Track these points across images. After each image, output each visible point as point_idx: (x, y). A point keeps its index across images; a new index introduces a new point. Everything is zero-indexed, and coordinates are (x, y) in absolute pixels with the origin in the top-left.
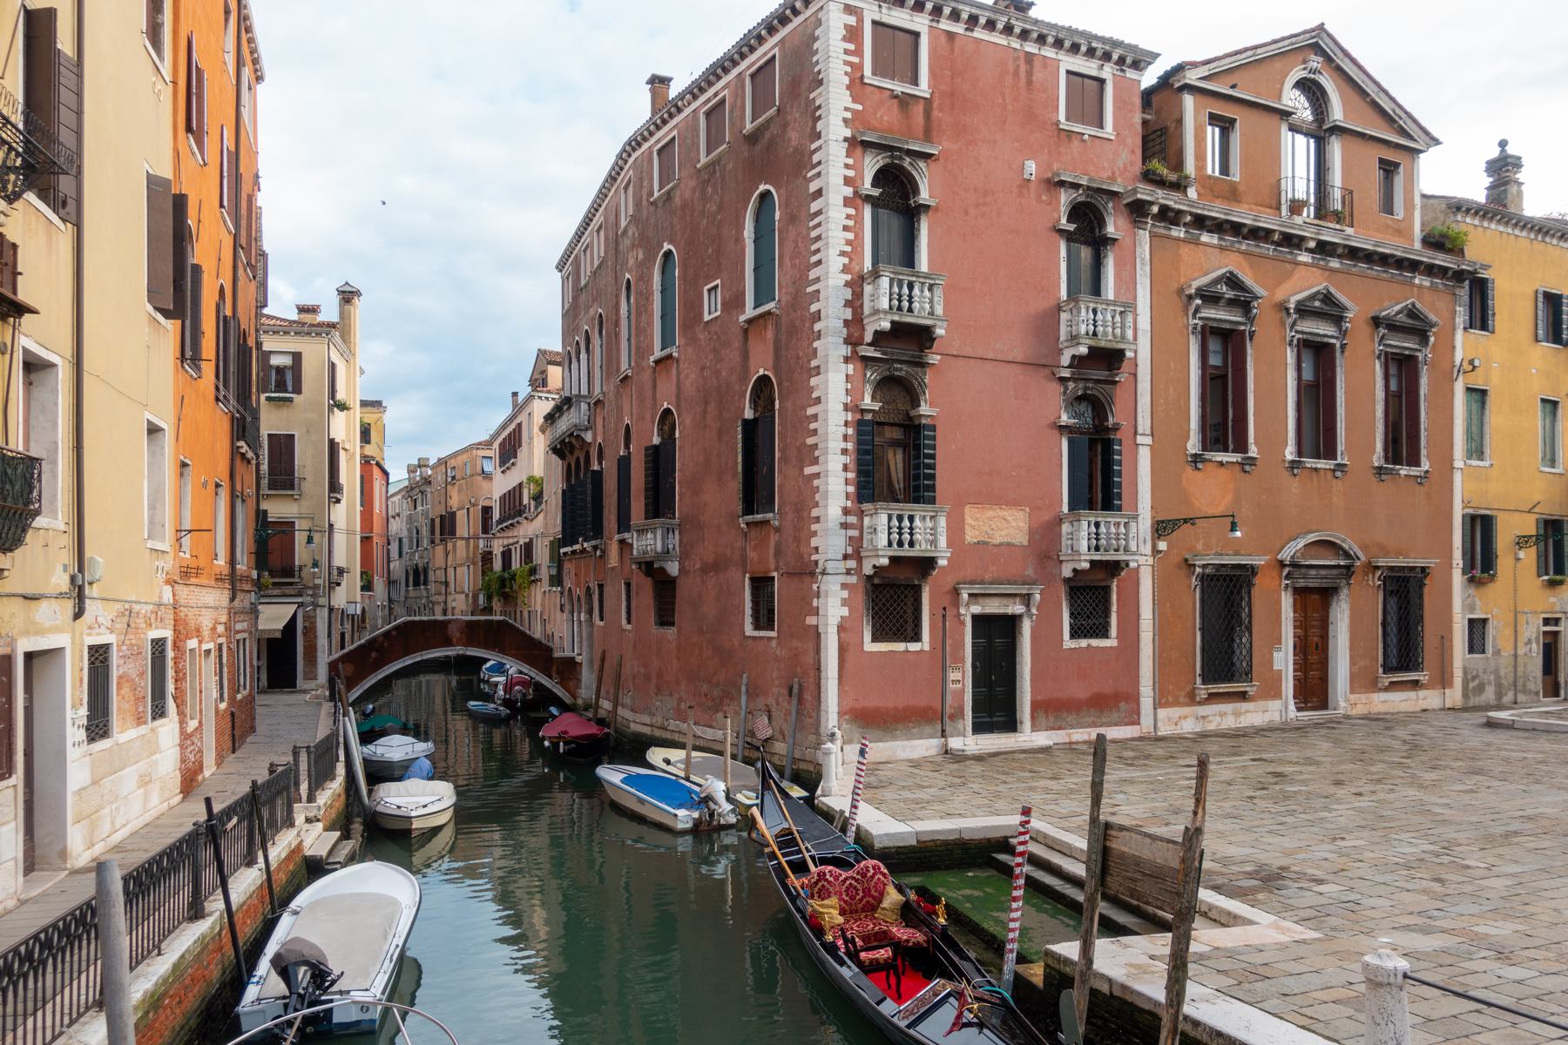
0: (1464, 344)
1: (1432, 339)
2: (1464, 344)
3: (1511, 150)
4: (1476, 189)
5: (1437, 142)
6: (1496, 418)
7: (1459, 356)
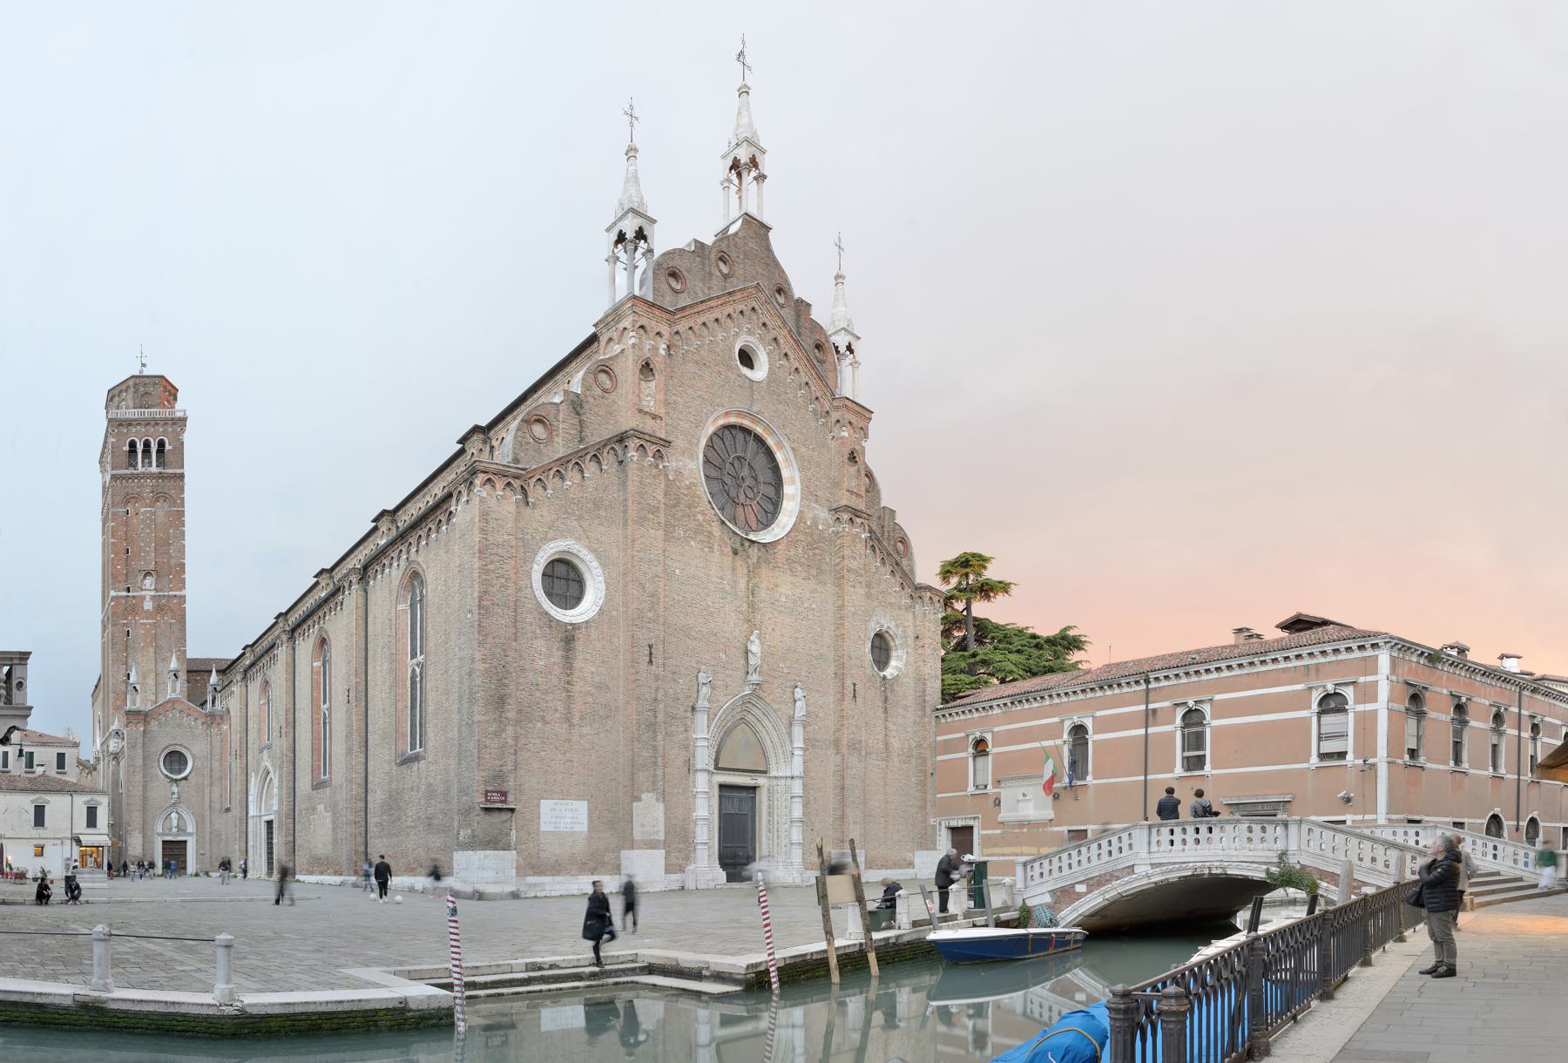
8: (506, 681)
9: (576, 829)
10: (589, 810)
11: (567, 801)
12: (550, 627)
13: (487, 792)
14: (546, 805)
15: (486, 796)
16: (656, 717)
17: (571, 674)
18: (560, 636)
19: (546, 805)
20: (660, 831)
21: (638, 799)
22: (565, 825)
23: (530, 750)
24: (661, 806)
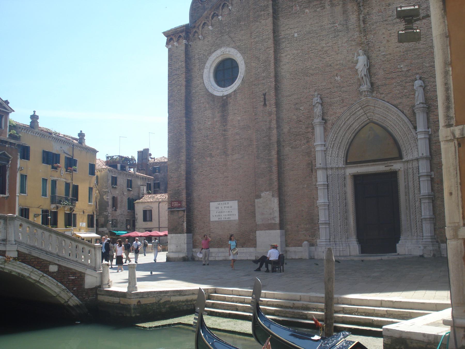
0: (20, 163)
1: (10, 162)
2: (20, 163)
3: (36, 114)
4: (28, 122)
5: (14, 111)
6: (29, 183)
7: (18, 166)
8: (181, 140)
9: (232, 219)
10: (239, 206)
11: (225, 202)
12: (214, 101)
13: (172, 202)
14: (213, 205)
15: (171, 204)
16: (270, 139)
17: (226, 125)
18: (219, 104)
19: (213, 205)
20: (276, 217)
21: (259, 197)
22: (224, 217)
23: (203, 175)
24: (276, 200)
